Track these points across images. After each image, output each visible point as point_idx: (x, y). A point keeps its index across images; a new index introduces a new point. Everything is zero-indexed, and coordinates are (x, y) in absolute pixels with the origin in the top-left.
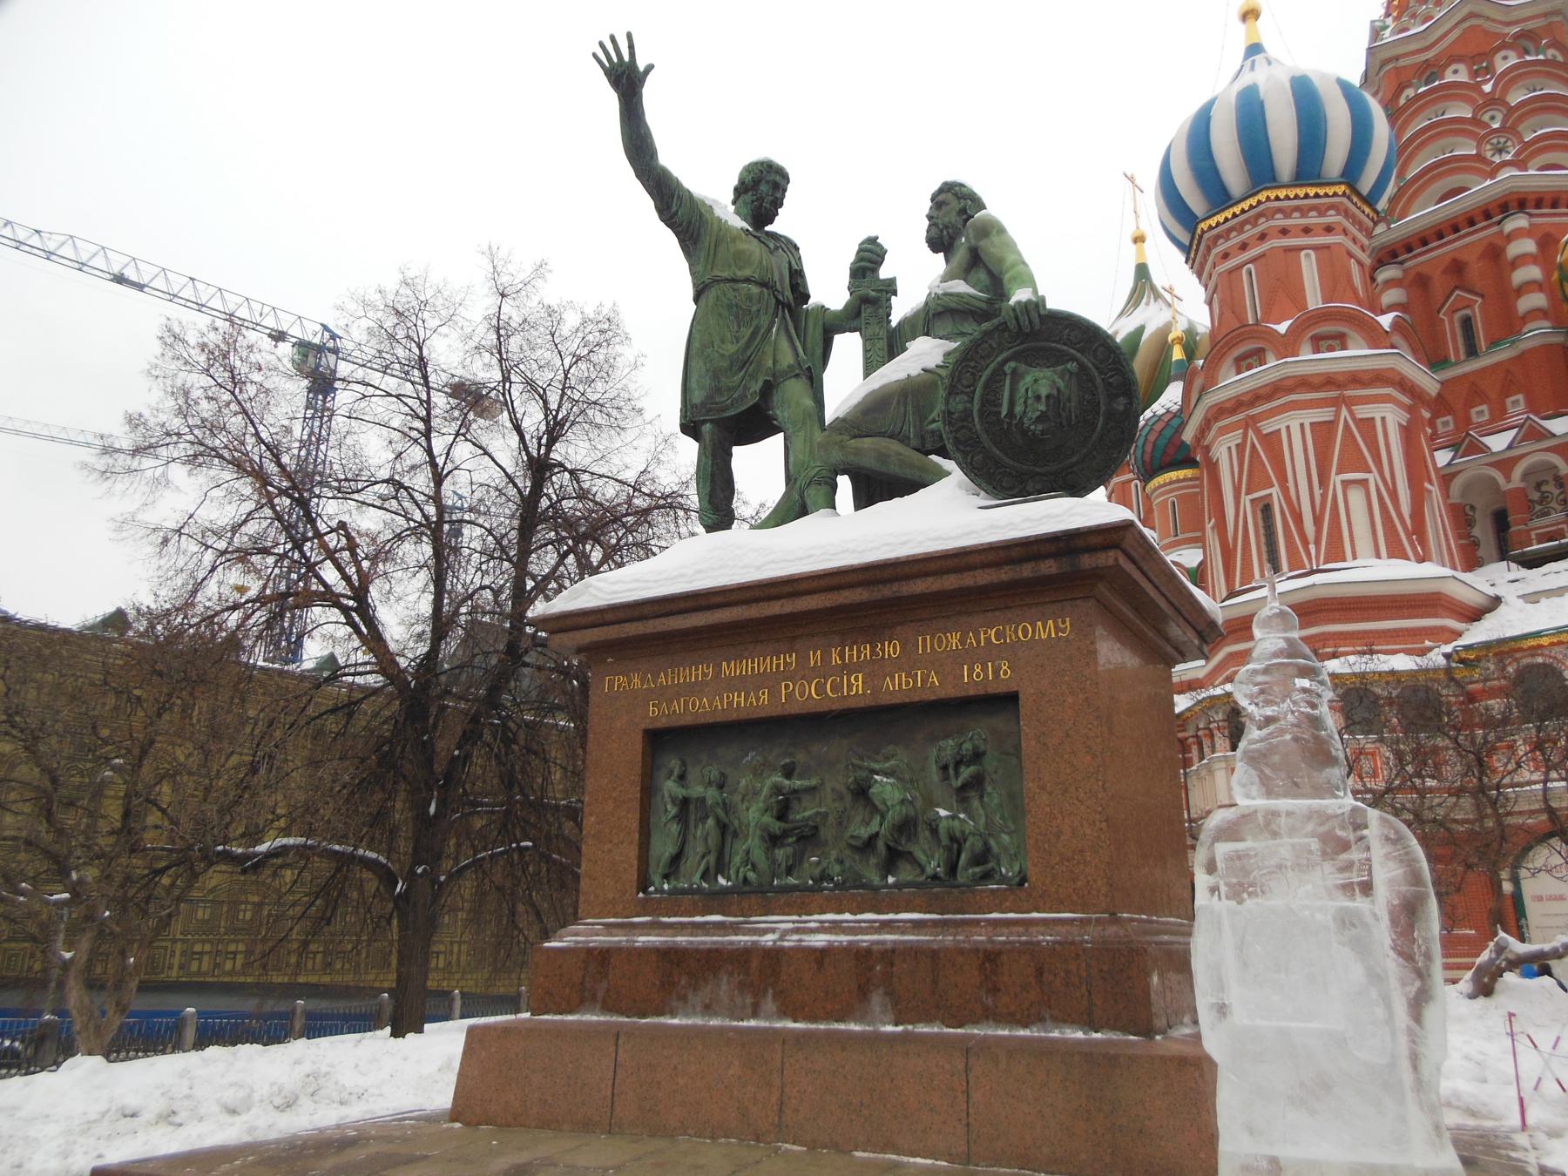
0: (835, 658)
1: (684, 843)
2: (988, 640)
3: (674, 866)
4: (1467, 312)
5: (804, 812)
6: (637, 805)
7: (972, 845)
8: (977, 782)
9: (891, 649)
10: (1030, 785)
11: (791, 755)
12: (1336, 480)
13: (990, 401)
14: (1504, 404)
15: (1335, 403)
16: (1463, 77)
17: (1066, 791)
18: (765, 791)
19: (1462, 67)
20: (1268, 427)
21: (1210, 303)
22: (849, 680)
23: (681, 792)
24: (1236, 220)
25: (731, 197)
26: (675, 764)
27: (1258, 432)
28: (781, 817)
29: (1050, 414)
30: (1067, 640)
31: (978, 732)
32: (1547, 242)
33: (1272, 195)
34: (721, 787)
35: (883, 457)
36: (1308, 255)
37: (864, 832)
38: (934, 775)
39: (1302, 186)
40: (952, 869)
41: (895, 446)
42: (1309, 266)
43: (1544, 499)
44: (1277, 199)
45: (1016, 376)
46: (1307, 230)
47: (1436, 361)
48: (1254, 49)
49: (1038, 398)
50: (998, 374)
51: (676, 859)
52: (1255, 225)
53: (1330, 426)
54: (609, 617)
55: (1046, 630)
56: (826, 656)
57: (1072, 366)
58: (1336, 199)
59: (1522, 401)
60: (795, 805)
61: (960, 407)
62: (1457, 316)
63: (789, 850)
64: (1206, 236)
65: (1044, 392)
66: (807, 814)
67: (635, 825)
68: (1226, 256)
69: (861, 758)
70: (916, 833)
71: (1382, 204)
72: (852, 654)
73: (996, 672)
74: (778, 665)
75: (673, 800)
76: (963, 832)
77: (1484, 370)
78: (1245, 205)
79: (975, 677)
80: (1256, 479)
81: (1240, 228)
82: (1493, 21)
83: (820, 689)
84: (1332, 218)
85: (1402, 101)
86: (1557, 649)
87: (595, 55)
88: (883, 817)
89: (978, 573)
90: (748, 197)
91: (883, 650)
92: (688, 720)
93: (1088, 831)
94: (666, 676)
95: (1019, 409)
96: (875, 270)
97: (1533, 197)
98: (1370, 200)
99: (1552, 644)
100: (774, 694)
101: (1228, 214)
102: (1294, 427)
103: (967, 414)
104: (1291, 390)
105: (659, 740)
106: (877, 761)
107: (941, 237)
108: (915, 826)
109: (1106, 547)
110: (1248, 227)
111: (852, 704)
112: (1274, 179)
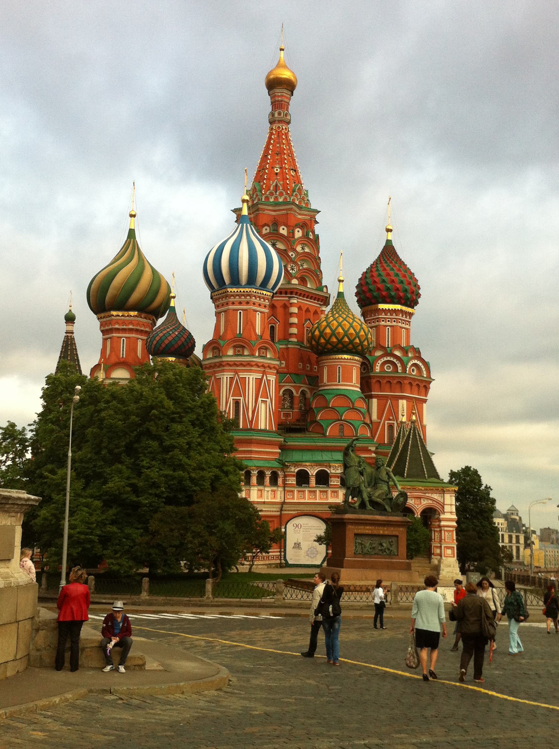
4: (274, 325)
5: (374, 545)
9: (386, 528)
12: (260, 399)
15: (264, 373)
19: (285, 228)
20: (242, 375)
27: (238, 376)
31: (394, 539)
32: (300, 308)
42: (258, 317)
46: (260, 305)
53: (261, 380)
55: (401, 529)
62: (270, 326)
68: (233, 303)
79: (395, 533)
80: (237, 392)
81: (240, 296)
97: (299, 292)
102: (252, 378)
104: (252, 366)
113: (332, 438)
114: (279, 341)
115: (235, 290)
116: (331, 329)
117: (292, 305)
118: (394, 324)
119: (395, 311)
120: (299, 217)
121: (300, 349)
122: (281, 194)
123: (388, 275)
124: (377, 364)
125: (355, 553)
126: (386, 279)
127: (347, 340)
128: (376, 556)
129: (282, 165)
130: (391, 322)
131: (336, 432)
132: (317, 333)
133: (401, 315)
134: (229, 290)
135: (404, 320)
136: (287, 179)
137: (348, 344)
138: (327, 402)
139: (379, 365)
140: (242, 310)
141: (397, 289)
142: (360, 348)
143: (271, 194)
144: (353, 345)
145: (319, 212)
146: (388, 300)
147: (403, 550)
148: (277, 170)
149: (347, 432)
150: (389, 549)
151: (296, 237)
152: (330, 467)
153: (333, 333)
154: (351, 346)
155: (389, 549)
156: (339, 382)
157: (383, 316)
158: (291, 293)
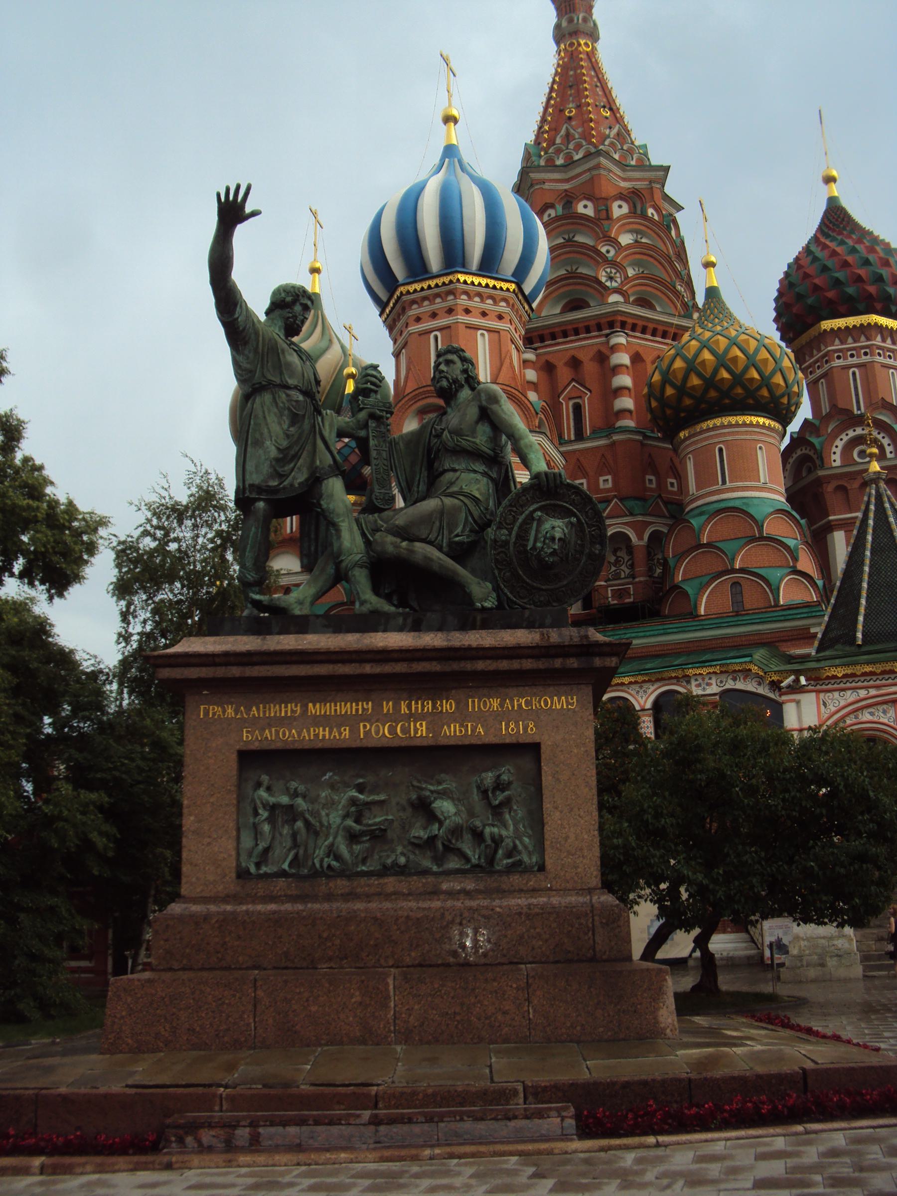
0: (404, 709)
1: (273, 838)
2: (520, 706)
3: (264, 857)
5: (376, 819)
6: (234, 809)
7: (508, 842)
8: (507, 802)
9: (448, 706)
10: (547, 805)
11: (361, 777)
13: (522, 536)
14: (598, 480)
16: (590, 212)
17: (571, 810)
18: (343, 802)
21: (397, 355)
22: (415, 726)
23: (272, 800)
24: (430, 292)
25: (266, 304)
26: (265, 779)
28: (358, 821)
29: (558, 551)
30: (574, 711)
32: (637, 358)
33: (462, 278)
34: (304, 797)
35: (427, 559)
36: (482, 335)
37: (423, 834)
38: (475, 796)
39: (484, 276)
40: (491, 861)
41: (435, 554)
43: (617, 562)
44: (465, 282)
45: (540, 522)
47: (560, 440)
48: (450, 151)
49: (553, 539)
50: (530, 518)
51: (266, 850)
52: (444, 300)
54: (217, 660)
56: (397, 707)
57: (574, 520)
58: (507, 294)
59: (610, 481)
60: (367, 813)
61: (503, 538)
62: (571, 403)
63: (367, 845)
64: (404, 298)
65: (558, 535)
66: (378, 820)
67: (232, 825)
68: (418, 319)
69: (419, 781)
70: (462, 837)
71: (534, 305)
72: (417, 706)
73: (525, 728)
74: (357, 710)
75: (265, 806)
76: (501, 836)
77: (587, 449)
78: (440, 281)
79: (510, 731)
81: (430, 299)
82: (615, 174)
83: (392, 730)
84: (502, 307)
85: (546, 218)
86: (633, 686)
87: (219, 195)
88: (441, 824)
89: (524, 661)
90: (286, 313)
91: (442, 706)
92: (279, 745)
93: (586, 837)
94: (258, 709)
95: (539, 545)
96: (376, 392)
97: (630, 321)
98: (528, 300)
99: (631, 683)
100: (354, 731)
101: (425, 285)
103: (506, 543)
105: (249, 759)
106: (431, 784)
107: (450, 388)
108: (461, 831)
109: (611, 655)
110: (438, 300)
111: (418, 743)
112: (464, 266)
113: (717, 620)
114: (593, 432)
115: (418, 286)
116: (685, 359)
117: (614, 349)
118: (864, 359)
119: (865, 330)
120: (623, 184)
121: (641, 442)
122: (578, 147)
123: (834, 253)
124: (834, 449)
125: (242, 874)
126: (829, 263)
127: (725, 375)
128: (391, 883)
129: (580, 100)
130: (859, 356)
131: (726, 603)
132: (657, 377)
133: (879, 338)
134: (402, 289)
135: (889, 350)
136: (591, 120)
137: (732, 387)
138: (696, 534)
139: (838, 451)
140: (440, 329)
141: (859, 279)
142: (765, 392)
143: (558, 151)
144: (744, 387)
145: (667, 169)
146: (842, 309)
147: (573, 826)
148: (571, 112)
149: (751, 600)
150: (478, 836)
151: (615, 217)
152: (688, 682)
153: (692, 367)
154: (739, 390)
155: (478, 836)
156: (724, 482)
157: (837, 345)
158: (611, 325)
